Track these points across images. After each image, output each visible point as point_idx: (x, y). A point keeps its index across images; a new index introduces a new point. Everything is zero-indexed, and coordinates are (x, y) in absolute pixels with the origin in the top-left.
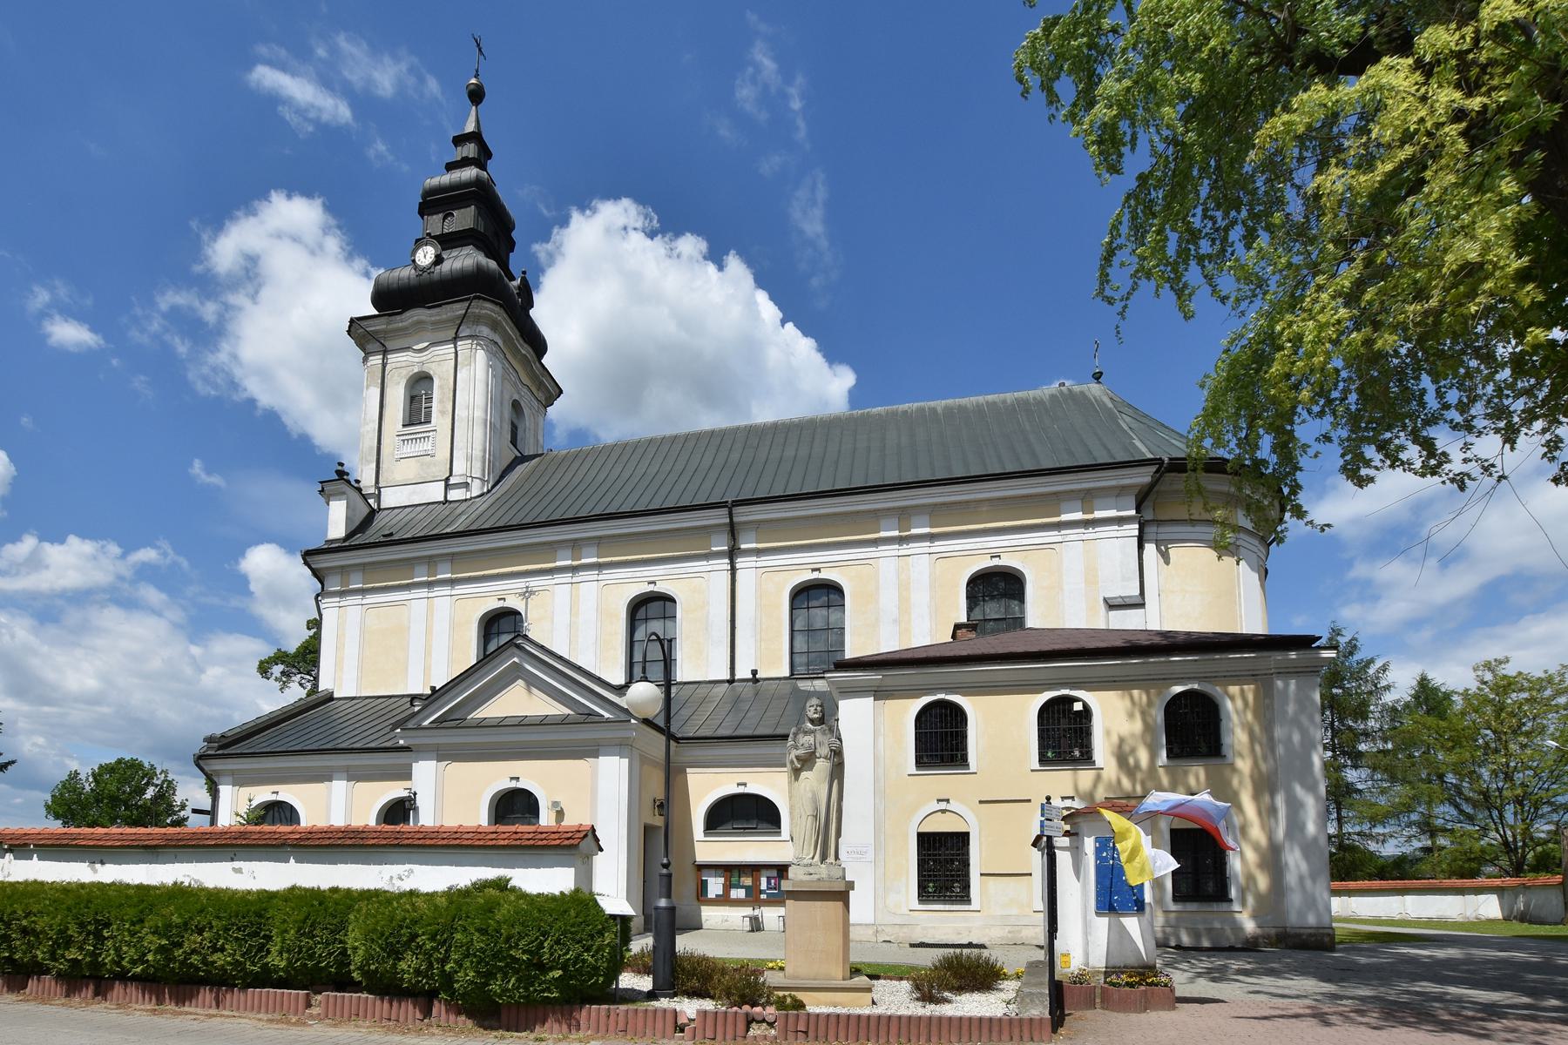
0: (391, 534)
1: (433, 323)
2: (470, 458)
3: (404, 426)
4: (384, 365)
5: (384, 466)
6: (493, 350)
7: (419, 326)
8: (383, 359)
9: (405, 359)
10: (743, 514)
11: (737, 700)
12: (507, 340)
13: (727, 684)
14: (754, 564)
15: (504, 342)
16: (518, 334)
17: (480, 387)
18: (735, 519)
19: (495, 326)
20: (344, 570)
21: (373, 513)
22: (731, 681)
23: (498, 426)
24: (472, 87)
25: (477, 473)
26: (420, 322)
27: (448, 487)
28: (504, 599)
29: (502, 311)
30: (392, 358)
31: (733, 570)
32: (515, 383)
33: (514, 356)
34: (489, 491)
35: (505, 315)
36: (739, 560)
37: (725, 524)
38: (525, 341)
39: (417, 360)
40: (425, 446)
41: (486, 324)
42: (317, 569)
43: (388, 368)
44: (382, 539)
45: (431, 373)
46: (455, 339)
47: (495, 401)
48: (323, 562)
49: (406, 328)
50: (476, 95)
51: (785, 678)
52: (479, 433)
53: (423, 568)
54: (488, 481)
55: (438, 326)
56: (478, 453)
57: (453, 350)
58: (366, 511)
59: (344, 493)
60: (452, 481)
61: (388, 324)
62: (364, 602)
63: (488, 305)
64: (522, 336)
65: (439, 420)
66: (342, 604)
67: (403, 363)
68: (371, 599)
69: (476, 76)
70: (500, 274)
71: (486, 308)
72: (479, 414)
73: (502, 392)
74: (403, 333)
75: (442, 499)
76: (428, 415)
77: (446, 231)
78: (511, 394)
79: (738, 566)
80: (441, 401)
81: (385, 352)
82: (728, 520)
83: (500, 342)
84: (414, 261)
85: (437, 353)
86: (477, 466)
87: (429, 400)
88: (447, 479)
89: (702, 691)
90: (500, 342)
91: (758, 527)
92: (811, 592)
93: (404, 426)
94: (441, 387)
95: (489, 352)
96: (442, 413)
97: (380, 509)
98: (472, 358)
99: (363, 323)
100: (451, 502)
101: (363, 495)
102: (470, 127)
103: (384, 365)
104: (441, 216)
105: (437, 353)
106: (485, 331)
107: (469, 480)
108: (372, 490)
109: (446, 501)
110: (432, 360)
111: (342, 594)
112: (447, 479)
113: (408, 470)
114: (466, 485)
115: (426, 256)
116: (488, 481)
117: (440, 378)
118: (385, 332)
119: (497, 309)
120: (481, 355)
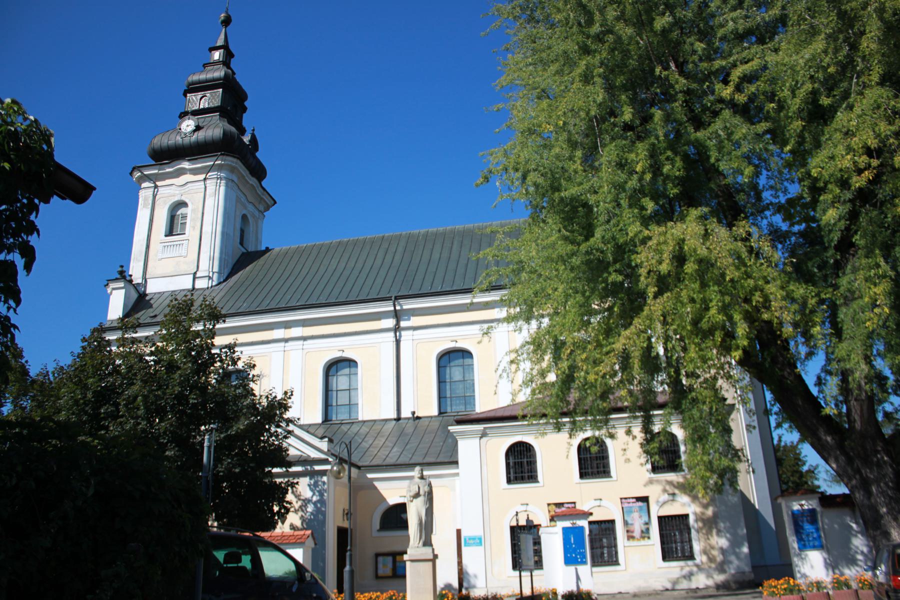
0: (155, 316)
4: (154, 196)
11: (402, 433)
13: (394, 422)
16: (248, 172)
22: (398, 419)
25: (216, 269)
31: (398, 342)
39: (177, 192)
43: (157, 197)
44: (149, 320)
45: (187, 201)
51: (435, 417)
57: (203, 186)
60: (198, 275)
64: (251, 173)
65: (192, 232)
77: (202, 107)
82: (392, 308)
88: (195, 273)
89: (377, 427)
90: (235, 178)
92: (451, 355)
93: (166, 236)
100: (198, 289)
101: (134, 285)
103: (154, 196)
105: (191, 188)
108: (140, 281)
112: (195, 273)
113: (167, 266)
115: (188, 125)
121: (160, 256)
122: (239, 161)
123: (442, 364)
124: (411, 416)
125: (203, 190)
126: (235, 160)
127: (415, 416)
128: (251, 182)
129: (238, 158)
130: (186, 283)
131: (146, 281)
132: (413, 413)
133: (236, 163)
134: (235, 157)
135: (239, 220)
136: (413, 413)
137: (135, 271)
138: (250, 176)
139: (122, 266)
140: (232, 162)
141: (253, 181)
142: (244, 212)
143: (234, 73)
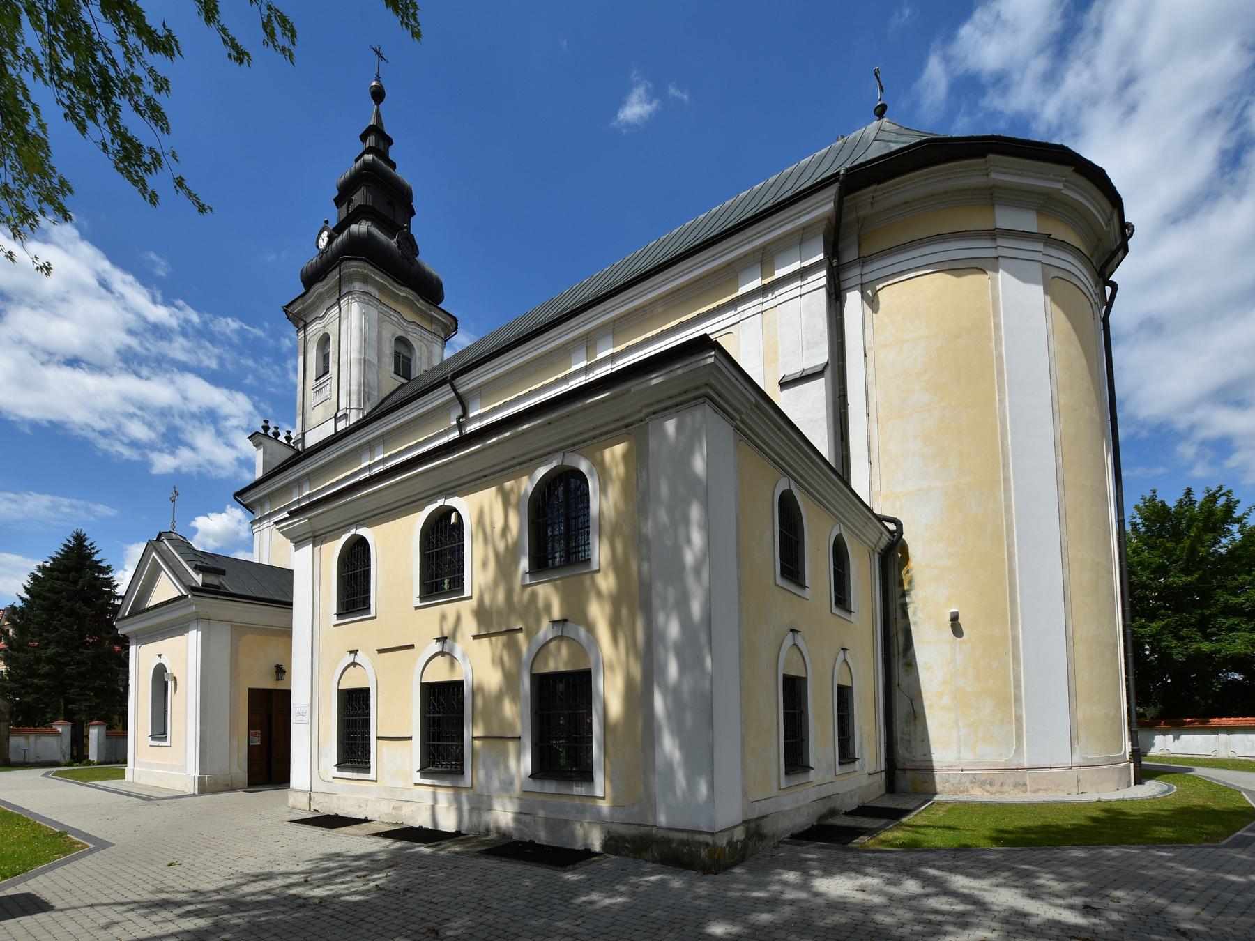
2: (349, 394)
8: (305, 333)
9: (316, 327)
16: (391, 281)
17: (356, 333)
18: (459, 391)
19: (365, 280)
24: (374, 88)
26: (321, 294)
27: (337, 419)
29: (366, 265)
32: (400, 324)
35: (370, 267)
37: (451, 401)
38: (402, 285)
39: (321, 325)
40: (326, 392)
41: (359, 280)
46: (339, 300)
49: (313, 303)
52: (355, 371)
54: (363, 409)
56: (354, 388)
60: (339, 415)
61: (303, 303)
63: (354, 263)
69: (378, 78)
71: (352, 267)
72: (355, 355)
78: (390, 332)
81: (305, 326)
84: (318, 247)
85: (330, 316)
86: (354, 398)
88: (336, 415)
93: (316, 380)
94: (333, 342)
98: (349, 310)
105: (330, 316)
106: (358, 286)
110: (330, 321)
114: (345, 416)
116: (363, 409)
117: (333, 335)
118: (304, 310)
119: (361, 264)
121: (314, 404)
125: (338, 315)
143: (393, 166)
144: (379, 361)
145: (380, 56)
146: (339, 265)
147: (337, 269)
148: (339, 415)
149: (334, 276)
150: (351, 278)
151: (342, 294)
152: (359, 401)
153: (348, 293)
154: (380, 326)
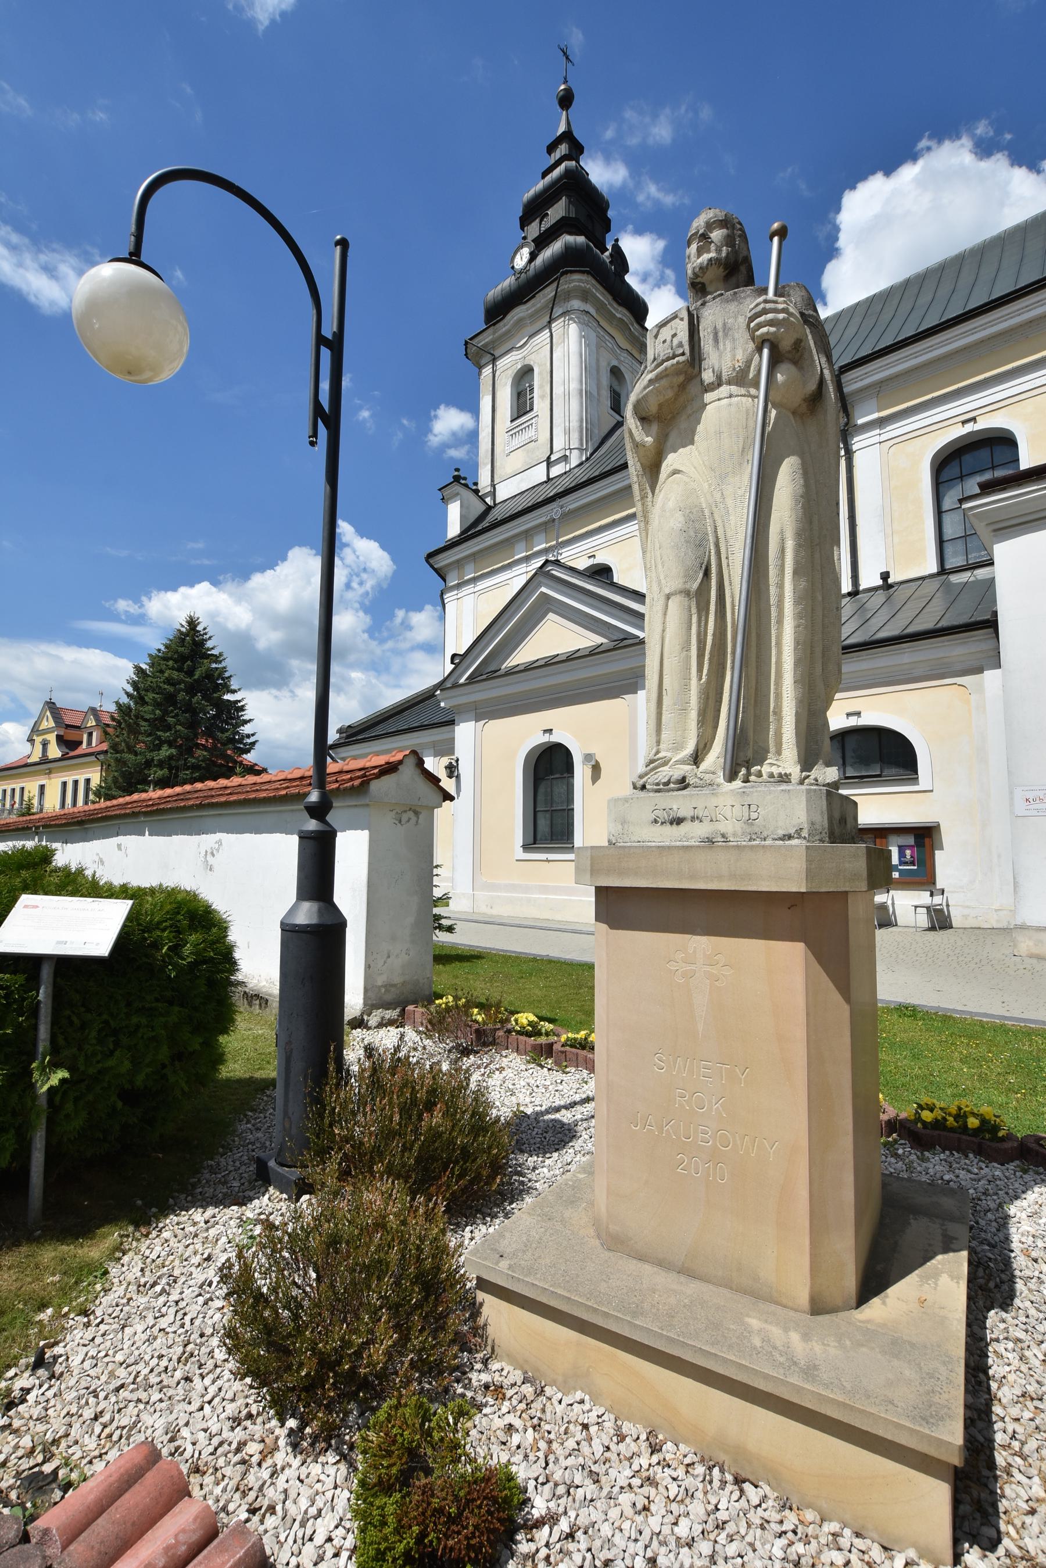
1: (531, 316)
2: (568, 432)
3: (512, 421)
5: (497, 464)
6: (586, 320)
7: (520, 324)
10: (856, 380)
12: (600, 307)
14: (877, 439)
15: (597, 310)
16: (610, 298)
17: (574, 360)
19: (585, 296)
20: (459, 564)
21: (489, 508)
23: (595, 394)
25: (575, 444)
26: (521, 320)
27: (549, 464)
28: (594, 556)
30: (501, 363)
32: (613, 351)
33: (611, 323)
34: (587, 459)
36: (856, 439)
38: (620, 304)
39: (520, 356)
40: (530, 433)
41: (576, 297)
42: (440, 569)
45: (532, 363)
47: (590, 370)
48: (442, 561)
49: (508, 332)
50: (566, 101)
52: (575, 404)
53: (522, 545)
54: (586, 450)
55: (534, 316)
56: (574, 424)
58: (482, 508)
59: (457, 494)
60: (553, 458)
61: (494, 333)
62: (477, 589)
63: (576, 276)
64: (615, 299)
65: (540, 405)
66: (459, 596)
67: (509, 364)
68: (482, 585)
69: (565, 82)
70: (588, 246)
71: (573, 281)
72: (574, 386)
73: (598, 360)
74: (508, 335)
75: (545, 479)
76: (532, 404)
78: (607, 360)
79: (855, 448)
80: (541, 387)
81: (494, 360)
83: (592, 311)
84: (513, 267)
86: (575, 436)
87: (532, 390)
88: (549, 458)
90: (592, 311)
91: (879, 390)
93: (512, 421)
94: (540, 373)
95: (581, 324)
96: (542, 397)
97: (495, 505)
98: (565, 334)
99: (474, 342)
102: (562, 128)
104: (538, 220)
106: (576, 304)
107: (568, 453)
109: (549, 480)
111: (458, 586)
114: (565, 458)
116: (586, 450)
117: (540, 366)
118: (493, 342)
120: (573, 329)
121: (508, 450)
122: (590, 278)
123: (945, 475)
124: (880, 582)
125: (548, 340)
126: (584, 277)
127: (890, 581)
128: (618, 315)
129: (588, 273)
130: (539, 474)
131: (493, 486)
132: (885, 576)
133: (587, 282)
134: (583, 272)
135: (605, 379)
136: (885, 576)
137: (484, 482)
138: (615, 305)
139: (457, 470)
140: (580, 281)
141: (621, 313)
142: (615, 363)
144: (598, 394)
145: (567, 58)
146: (558, 279)
147: (555, 285)
148: (553, 458)
149: (549, 292)
150: (568, 296)
151: (554, 316)
152: (581, 440)
153: (564, 314)
154: (598, 353)
